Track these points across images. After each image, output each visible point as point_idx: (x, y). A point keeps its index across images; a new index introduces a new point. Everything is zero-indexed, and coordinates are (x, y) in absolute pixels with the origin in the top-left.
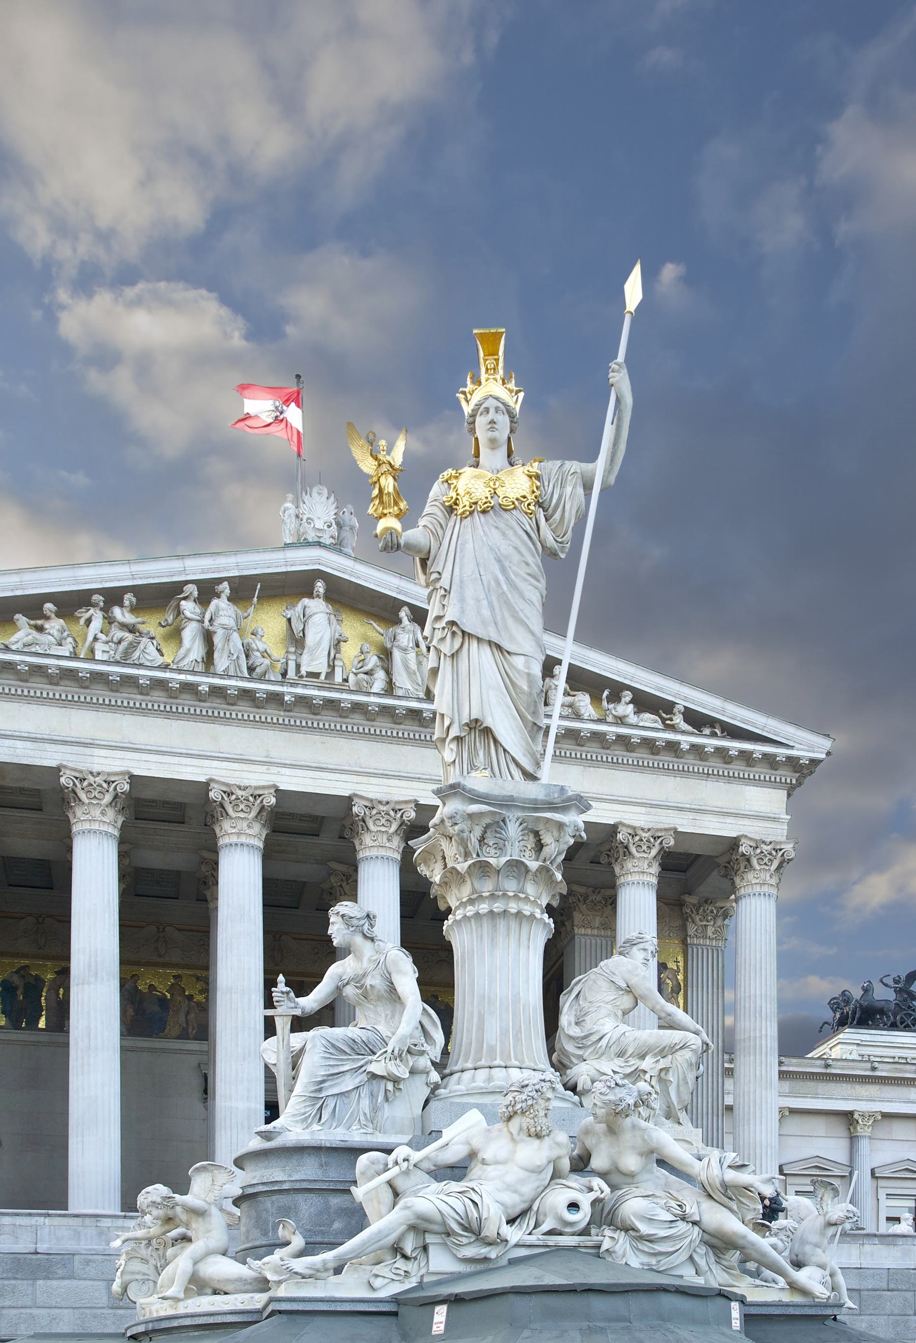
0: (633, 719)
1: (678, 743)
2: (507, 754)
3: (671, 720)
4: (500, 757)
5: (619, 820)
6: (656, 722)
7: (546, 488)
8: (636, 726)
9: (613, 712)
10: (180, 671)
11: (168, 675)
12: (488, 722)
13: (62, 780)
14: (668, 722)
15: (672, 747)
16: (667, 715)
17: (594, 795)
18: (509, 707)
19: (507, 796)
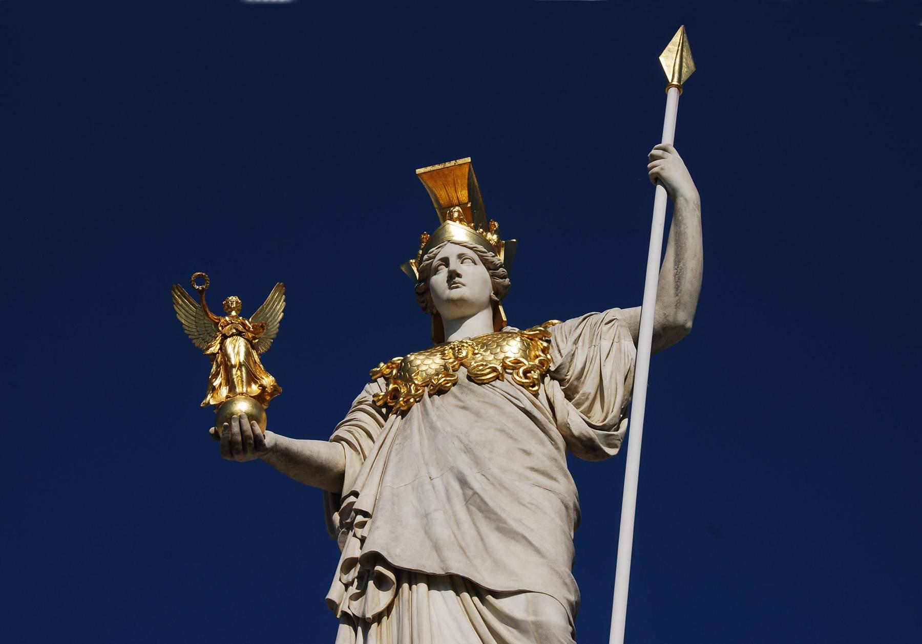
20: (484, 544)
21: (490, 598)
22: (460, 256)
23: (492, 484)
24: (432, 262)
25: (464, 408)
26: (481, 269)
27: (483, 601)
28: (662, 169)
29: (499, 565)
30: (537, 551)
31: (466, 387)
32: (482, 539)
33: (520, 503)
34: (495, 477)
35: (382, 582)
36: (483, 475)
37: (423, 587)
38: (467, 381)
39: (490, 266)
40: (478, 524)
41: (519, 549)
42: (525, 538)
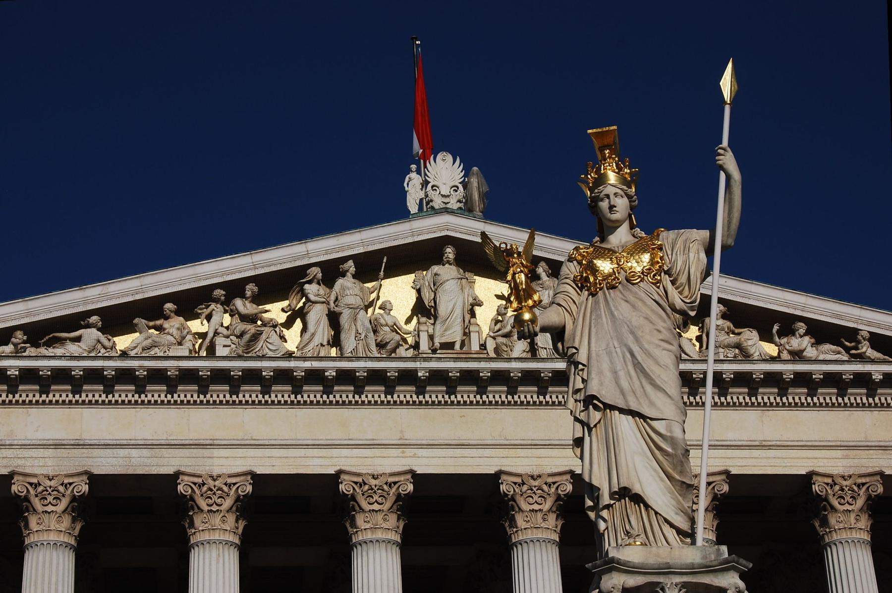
0: (811, 352)
1: (868, 375)
2: (659, 516)
3: (857, 348)
4: (652, 520)
5: (811, 469)
6: (839, 353)
7: (670, 257)
8: (816, 361)
9: (788, 347)
10: (304, 358)
11: (292, 364)
12: (637, 489)
13: (180, 488)
14: (853, 352)
15: (862, 380)
16: (851, 343)
17: (778, 443)
18: (655, 471)
19: (663, 564)
20: (644, 391)
21: (648, 420)
22: (616, 194)
23: (645, 353)
24: (599, 195)
25: (626, 301)
26: (626, 200)
27: (645, 421)
28: (724, 164)
29: (652, 404)
30: (670, 397)
31: (626, 286)
32: (643, 388)
33: (659, 365)
34: (646, 350)
35: (596, 408)
36: (640, 348)
37: (617, 412)
38: (625, 281)
39: (629, 197)
40: (641, 378)
41: (660, 395)
42: (664, 390)
